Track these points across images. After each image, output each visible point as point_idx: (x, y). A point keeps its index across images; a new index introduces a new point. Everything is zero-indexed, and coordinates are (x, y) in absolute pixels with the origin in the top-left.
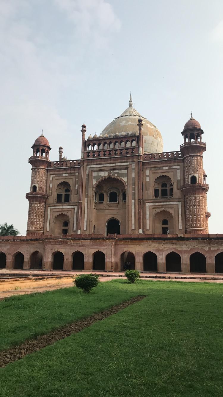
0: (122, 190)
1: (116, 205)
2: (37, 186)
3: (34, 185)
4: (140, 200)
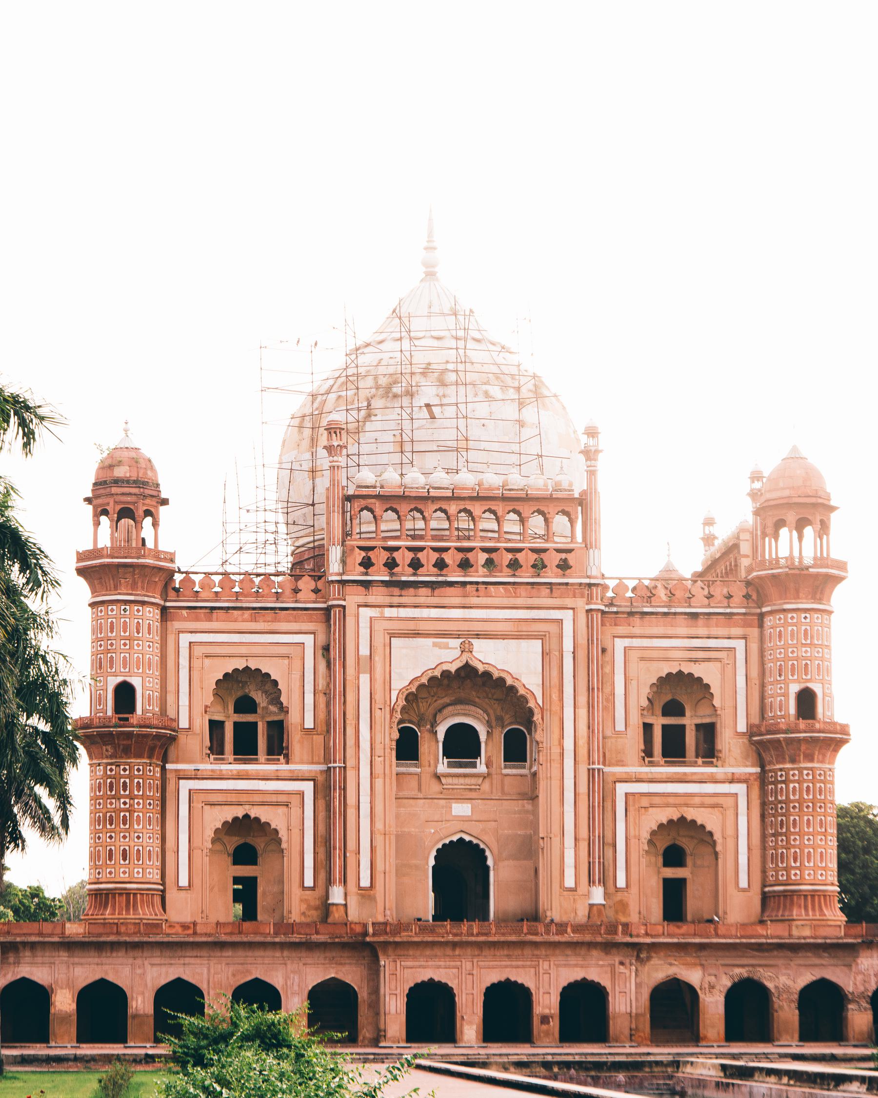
2: (136, 682)
3: (120, 679)
4: (599, 770)
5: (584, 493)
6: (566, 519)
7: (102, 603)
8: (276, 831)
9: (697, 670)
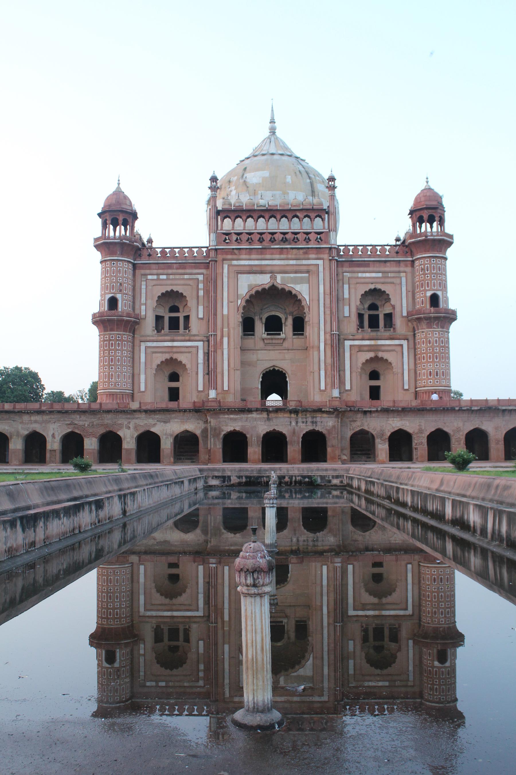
0: (291, 313)
1: (279, 341)
2: (119, 296)
4: (336, 334)
5: (328, 207)
6: (320, 219)
7: (105, 261)
8: (185, 365)
9: (383, 288)
